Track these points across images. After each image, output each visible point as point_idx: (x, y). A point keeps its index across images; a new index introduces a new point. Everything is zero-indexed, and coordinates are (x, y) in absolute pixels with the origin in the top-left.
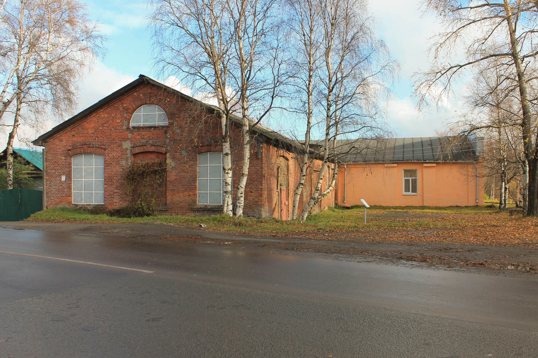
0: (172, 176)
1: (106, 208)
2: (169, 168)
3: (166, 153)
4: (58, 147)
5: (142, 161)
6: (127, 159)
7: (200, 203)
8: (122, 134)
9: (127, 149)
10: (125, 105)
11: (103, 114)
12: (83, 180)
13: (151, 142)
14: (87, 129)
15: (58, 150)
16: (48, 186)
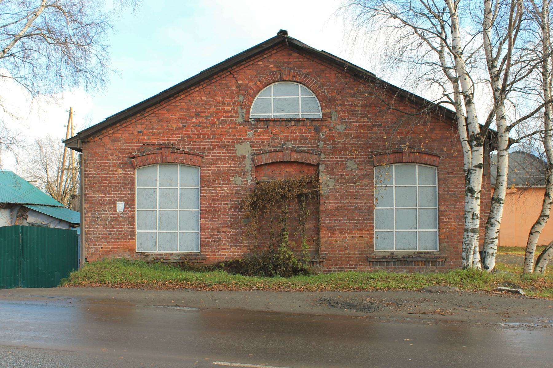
0: (328, 204)
1: (204, 259)
2: (323, 190)
3: (318, 165)
4: (109, 151)
5: (279, 176)
6: (244, 174)
7: (381, 248)
8: (235, 130)
9: (244, 157)
10: (240, 82)
11: (198, 97)
12: (158, 210)
13: (289, 145)
14: (168, 122)
15: (110, 157)
16: (89, 220)
